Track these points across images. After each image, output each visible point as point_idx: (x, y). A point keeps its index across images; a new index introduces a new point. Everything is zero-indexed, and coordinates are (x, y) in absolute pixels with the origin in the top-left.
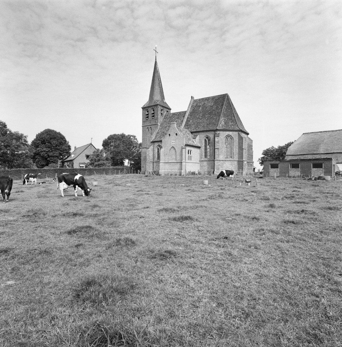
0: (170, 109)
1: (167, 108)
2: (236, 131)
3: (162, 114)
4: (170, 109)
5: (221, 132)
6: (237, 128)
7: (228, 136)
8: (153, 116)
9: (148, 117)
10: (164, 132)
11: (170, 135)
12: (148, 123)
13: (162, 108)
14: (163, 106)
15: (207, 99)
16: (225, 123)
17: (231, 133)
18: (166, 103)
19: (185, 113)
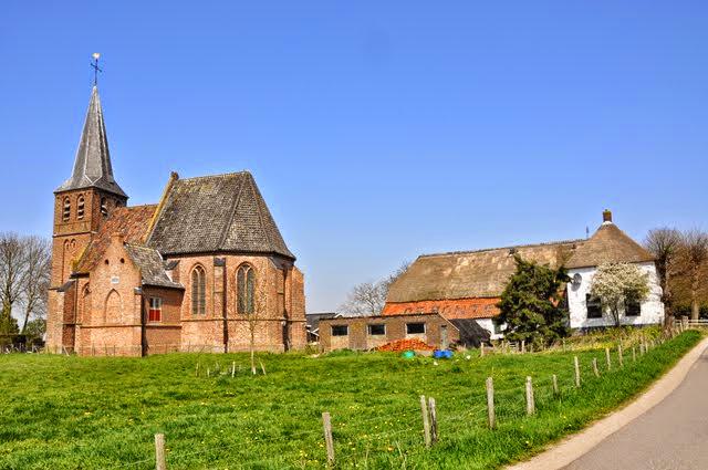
4: (126, 198)
7: (244, 265)
8: (81, 214)
9: (67, 215)
11: (107, 262)
12: (67, 230)
16: (240, 236)
18: (113, 183)
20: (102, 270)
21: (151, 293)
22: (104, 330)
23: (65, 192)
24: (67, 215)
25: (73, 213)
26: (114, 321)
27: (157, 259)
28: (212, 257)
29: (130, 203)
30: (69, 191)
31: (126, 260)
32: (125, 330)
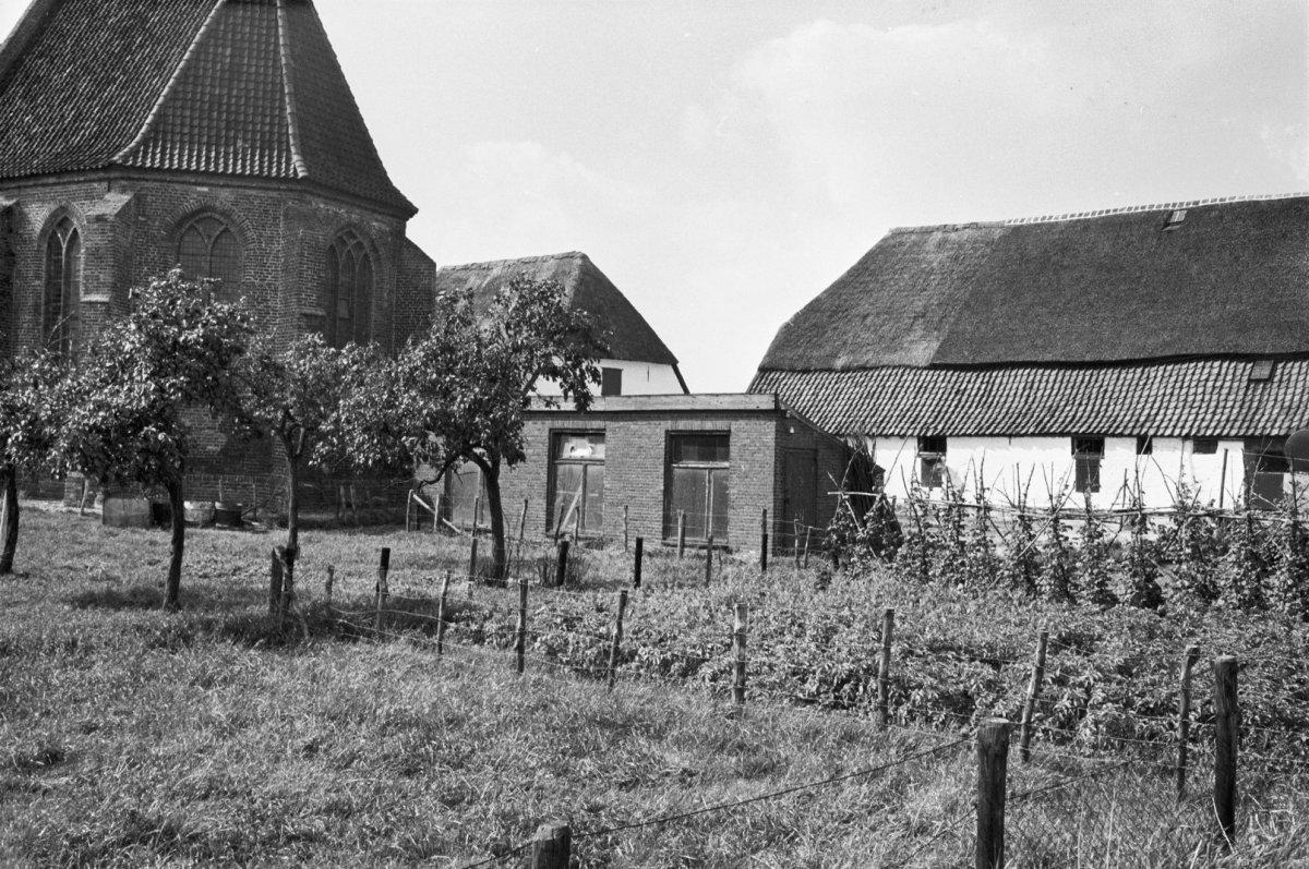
17: (225, 196)
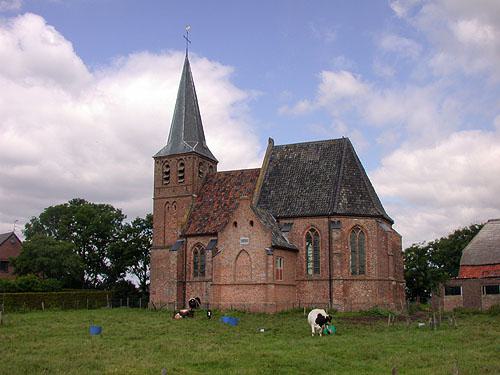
0: (216, 162)
1: (208, 159)
2: (372, 217)
3: (200, 173)
4: (216, 162)
5: (342, 219)
6: (373, 212)
7: (356, 228)
9: (167, 179)
10: (208, 215)
11: (235, 224)
12: (167, 192)
13: (201, 160)
14: (202, 157)
15: (305, 147)
16: (350, 201)
17: (362, 221)
19: (256, 172)
20: (230, 230)
21: (277, 253)
22: (235, 287)
23: (164, 157)
24: (167, 179)
25: (173, 176)
26: (244, 279)
27: (273, 221)
28: (326, 220)
29: (220, 168)
30: (170, 156)
31: (255, 222)
32: (257, 288)
